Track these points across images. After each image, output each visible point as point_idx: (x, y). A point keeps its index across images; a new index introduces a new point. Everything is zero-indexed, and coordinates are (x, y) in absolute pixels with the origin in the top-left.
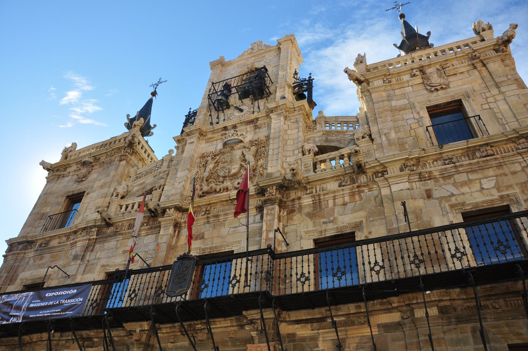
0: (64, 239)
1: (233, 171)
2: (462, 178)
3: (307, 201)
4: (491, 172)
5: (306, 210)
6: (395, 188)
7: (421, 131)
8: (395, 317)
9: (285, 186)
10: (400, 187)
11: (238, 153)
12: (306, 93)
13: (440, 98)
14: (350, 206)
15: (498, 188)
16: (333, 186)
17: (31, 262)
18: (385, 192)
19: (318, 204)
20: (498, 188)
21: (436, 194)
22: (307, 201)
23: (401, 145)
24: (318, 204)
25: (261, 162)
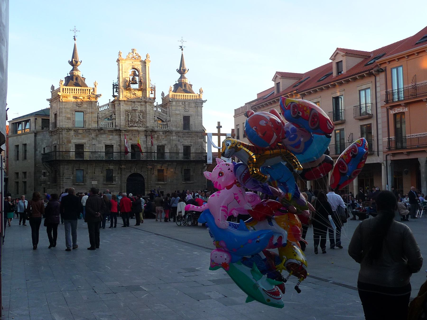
0: (84, 131)
1: (137, 121)
2: (185, 138)
3: (156, 136)
4: (190, 138)
5: (156, 138)
6: (174, 138)
7: (180, 123)
8: (170, 163)
9: (153, 131)
10: (174, 138)
11: (137, 114)
12: (153, 92)
13: (186, 114)
14: (164, 139)
15: (190, 142)
16: (161, 133)
17: (74, 136)
18: (171, 138)
19: (158, 137)
20: (190, 142)
21: (180, 141)
22: (156, 136)
23: (176, 127)
24: (158, 137)
25: (144, 120)
